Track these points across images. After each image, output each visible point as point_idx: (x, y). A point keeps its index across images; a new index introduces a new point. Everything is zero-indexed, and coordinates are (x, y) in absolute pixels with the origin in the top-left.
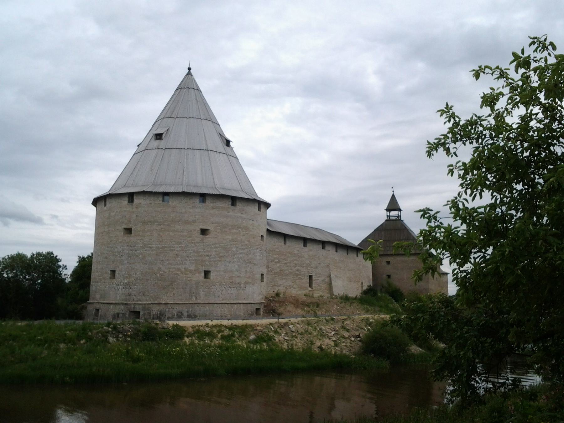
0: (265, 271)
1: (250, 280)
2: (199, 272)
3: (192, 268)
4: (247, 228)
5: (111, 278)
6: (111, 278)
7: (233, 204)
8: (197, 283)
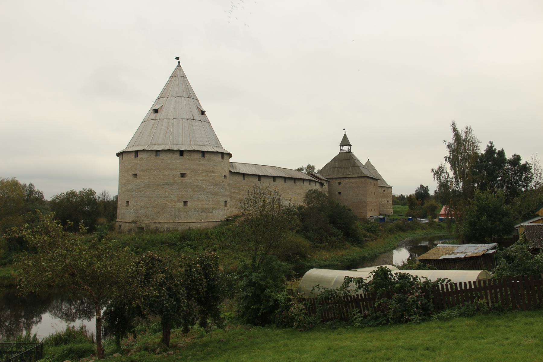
0: (228, 199)
1: (215, 206)
2: (181, 202)
3: (176, 199)
4: (213, 172)
5: (126, 206)
6: (126, 206)
7: (203, 156)
8: (179, 209)
